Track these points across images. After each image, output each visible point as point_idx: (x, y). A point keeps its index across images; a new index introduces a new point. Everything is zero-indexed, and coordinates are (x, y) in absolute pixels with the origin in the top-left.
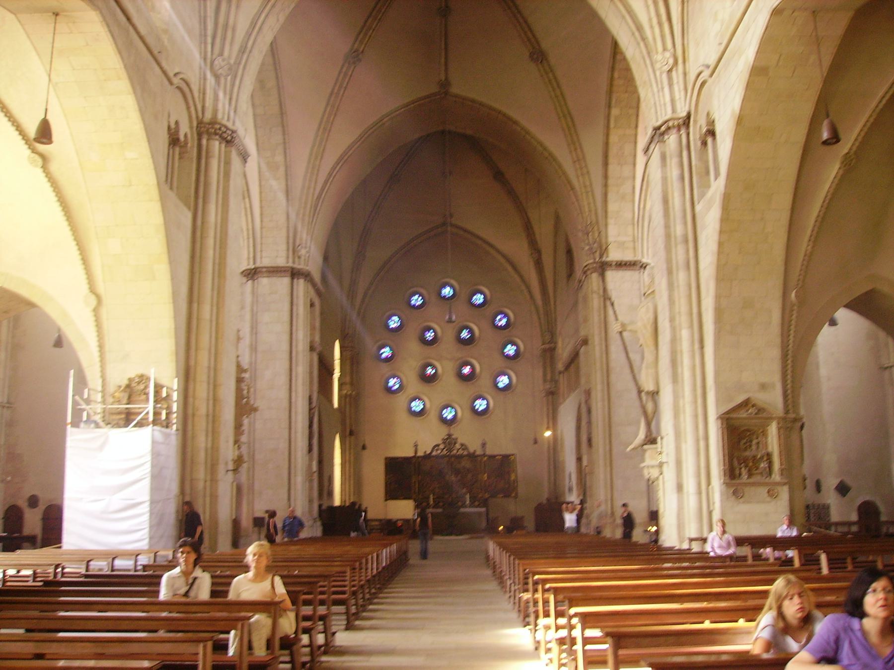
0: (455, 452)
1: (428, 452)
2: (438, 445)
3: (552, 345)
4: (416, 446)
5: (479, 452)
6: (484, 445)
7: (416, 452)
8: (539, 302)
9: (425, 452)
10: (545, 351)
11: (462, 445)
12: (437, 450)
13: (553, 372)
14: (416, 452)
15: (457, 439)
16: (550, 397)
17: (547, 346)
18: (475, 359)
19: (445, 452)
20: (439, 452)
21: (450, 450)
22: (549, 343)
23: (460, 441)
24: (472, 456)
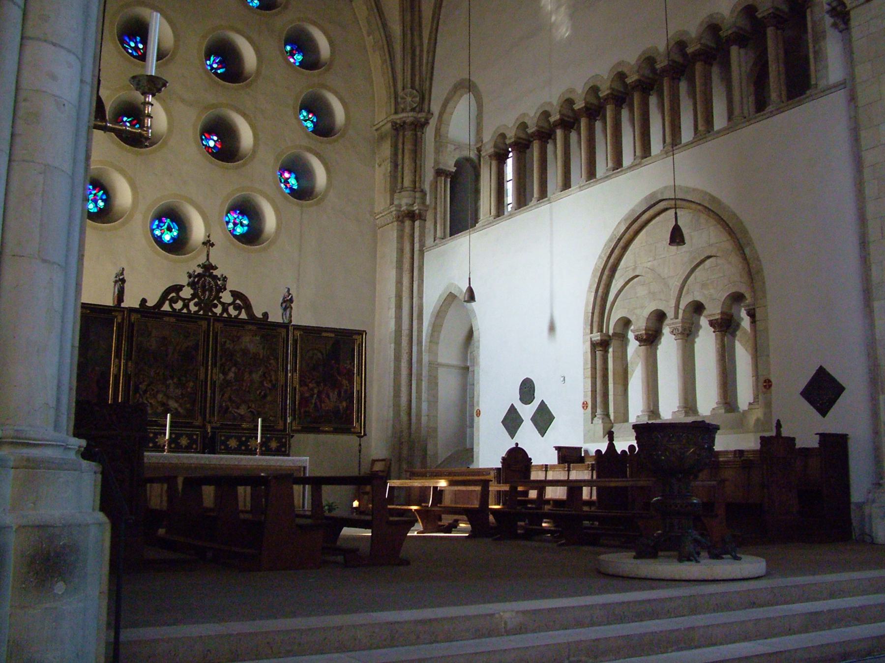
0: (218, 310)
1: (150, 303)
2: (178, 288)
3: (422, 116)
4: (120, 281)
5: (276, 316)
6: (287, 303)
7: (120, 297)
8: (396, 29)
9: (144, 301)
10: (398, 128)
11: (236, 295)
12: (173, 301)
13: (417, 170)
14: (120, 297)
15: (225, 279)
16: (408, 223)
17: (408, 116)
18: (244, 115)
19: (193, 308)
20: (178, 305)
21: (207, 306)
22: (413, 110)
23: (231, 286)
24: (263, 325)
